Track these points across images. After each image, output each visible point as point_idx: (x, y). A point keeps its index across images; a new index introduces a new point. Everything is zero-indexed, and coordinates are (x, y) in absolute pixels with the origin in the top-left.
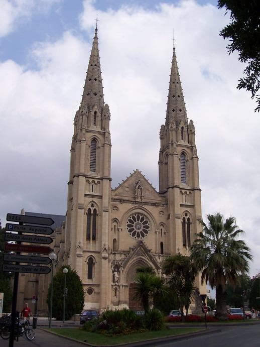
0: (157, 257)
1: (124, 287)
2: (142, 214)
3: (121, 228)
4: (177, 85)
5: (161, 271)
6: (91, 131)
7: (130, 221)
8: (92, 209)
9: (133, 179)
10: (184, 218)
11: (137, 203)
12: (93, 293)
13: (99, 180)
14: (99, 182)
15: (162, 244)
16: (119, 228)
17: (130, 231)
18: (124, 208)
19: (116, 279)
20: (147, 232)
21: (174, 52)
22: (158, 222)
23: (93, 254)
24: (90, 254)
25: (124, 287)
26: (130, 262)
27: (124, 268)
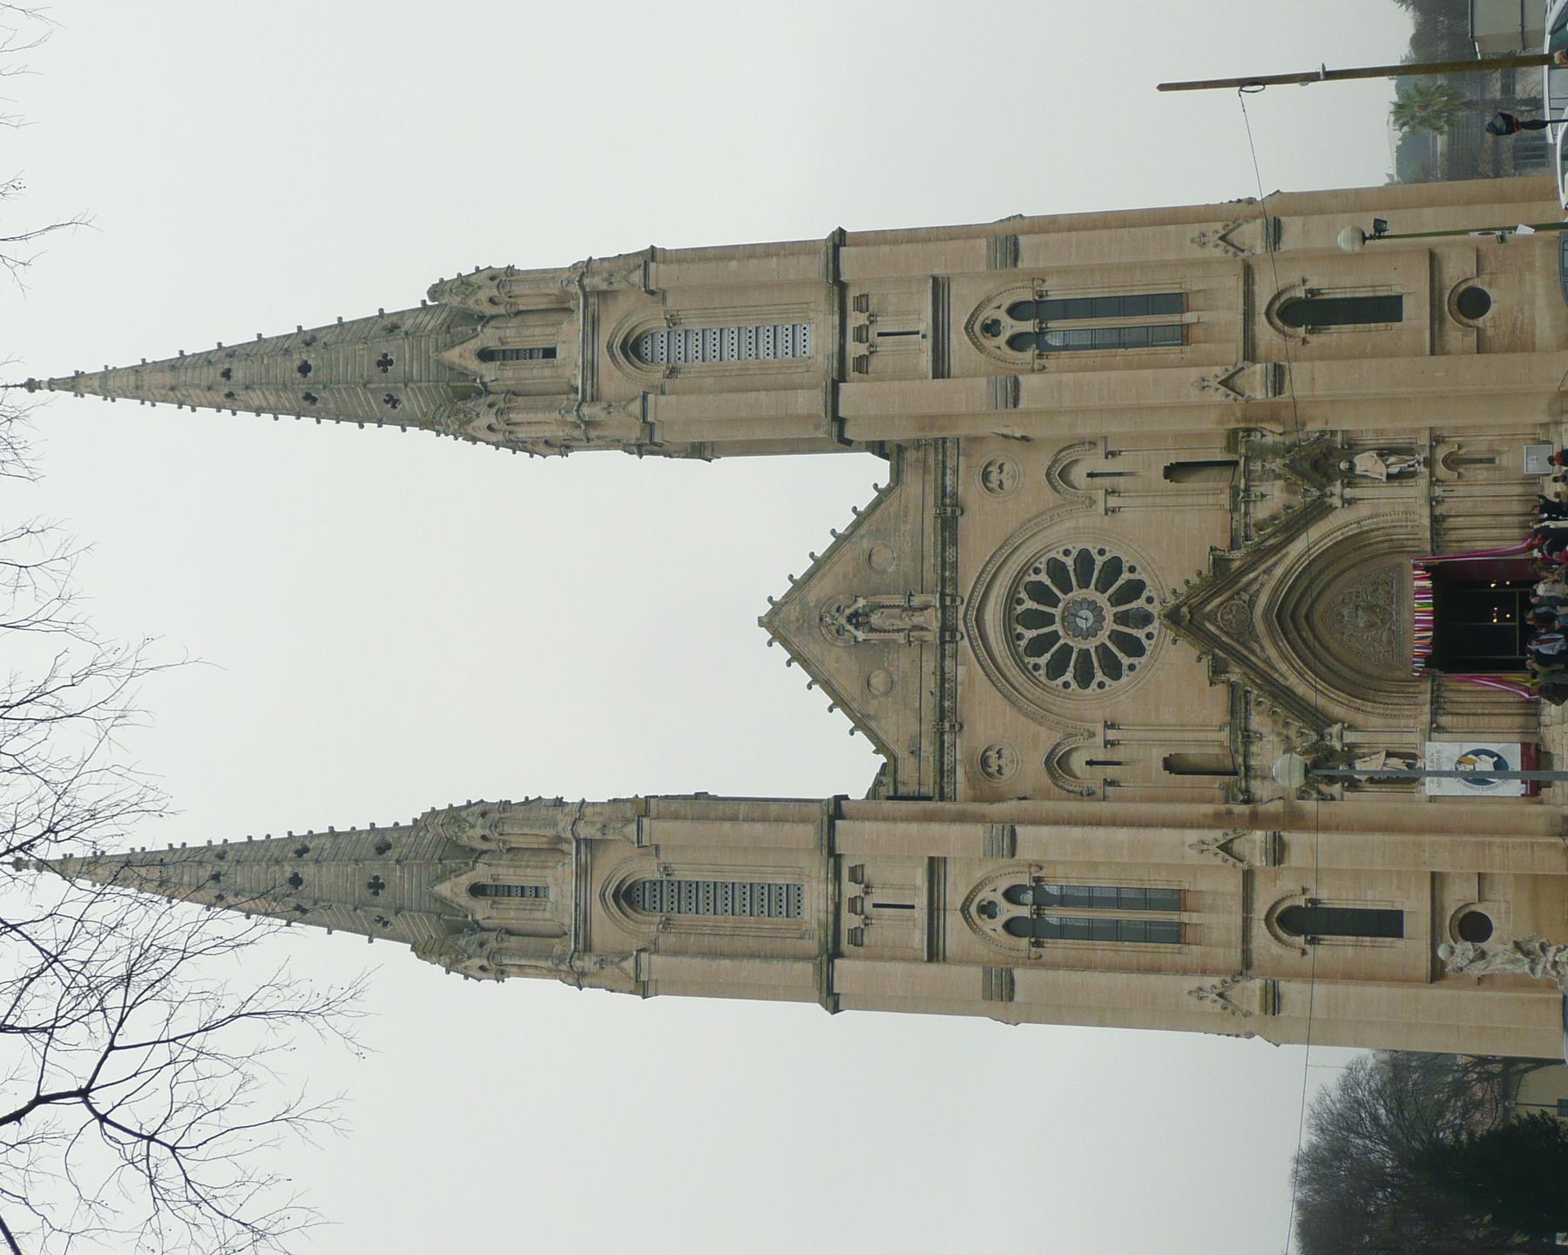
0: (1261, 512)
1: (1444, 720)
2: (1012, 599)
4: (238, 374)
5: (1337, 488)
6: (583, 919)
7: (1056, 669)
9: (813, 650)
10: (1016, 342)
11: (948, 631)
12: (1479, 908)
13: (845, 874)
14: (853, 870)
15: (1174, 472)
16: (1099, 740)
17: (1114, 670)
18: (989, 718)
21: (53, 384)
22: (1050, 498)
23: (1261, 909)
24: (1260, 930)
25: (1444, 720)
26: (1293, 681)
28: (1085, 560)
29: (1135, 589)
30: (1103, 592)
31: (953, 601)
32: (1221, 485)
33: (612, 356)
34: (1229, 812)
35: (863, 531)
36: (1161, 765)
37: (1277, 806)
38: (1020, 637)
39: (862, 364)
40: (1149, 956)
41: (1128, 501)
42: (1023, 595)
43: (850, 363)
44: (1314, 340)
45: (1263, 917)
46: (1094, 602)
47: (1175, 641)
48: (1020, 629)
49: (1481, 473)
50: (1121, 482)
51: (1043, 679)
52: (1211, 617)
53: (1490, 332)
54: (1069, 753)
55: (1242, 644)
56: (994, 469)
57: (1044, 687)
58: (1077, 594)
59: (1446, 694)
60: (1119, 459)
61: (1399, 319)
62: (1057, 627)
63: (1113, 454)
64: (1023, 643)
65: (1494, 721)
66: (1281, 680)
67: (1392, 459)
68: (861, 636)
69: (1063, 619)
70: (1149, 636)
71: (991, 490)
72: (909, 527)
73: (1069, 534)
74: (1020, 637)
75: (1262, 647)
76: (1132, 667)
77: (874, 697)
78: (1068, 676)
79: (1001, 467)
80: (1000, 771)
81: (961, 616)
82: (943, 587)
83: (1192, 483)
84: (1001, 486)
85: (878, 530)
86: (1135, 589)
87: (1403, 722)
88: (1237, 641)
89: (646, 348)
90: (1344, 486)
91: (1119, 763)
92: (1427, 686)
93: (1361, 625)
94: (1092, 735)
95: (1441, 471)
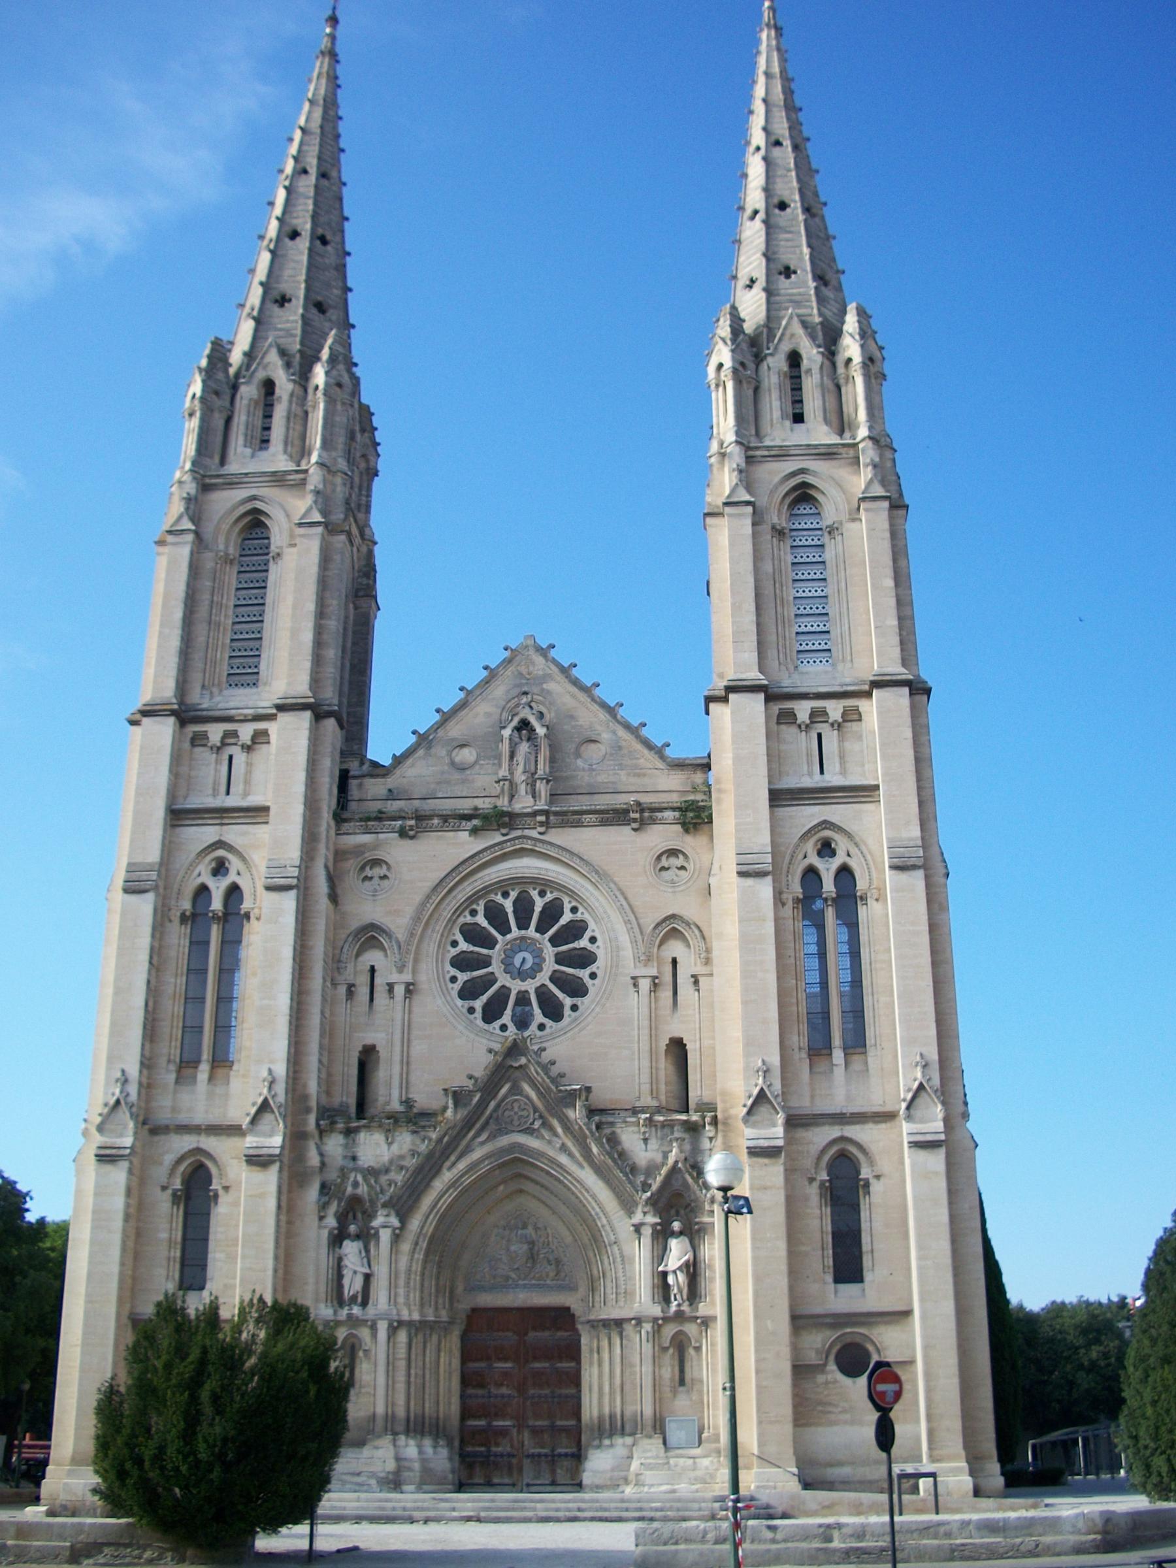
0: (630, 1138)
2: (544, 885)
3: (407, 977)
5: (652, 1219)
7: (473, 934)
8: (218, 888)
9: (500, 690)
15: (678, 1048)
16: (394, 977)
17: (468, 992)
19: (352, 1285)
20: (577, 990)
25: (402, 1336)
26: (447, 1176)
27: (403, 1218)
28: (585, 959)
29: (553, 1011)
30: (551, 979)
31: (542, 824)
32: (663, 1098)
33: (793, 474)
34: (308, 1110)
35: (622, 732)
36: (369, 1042)
37: (314, 1160)
38: (506, 895)
39: (787, 717)
40: (167, 1030)
41: (646, 1000)
42: (549, 897)
43: (788, 705)
44: (813, 1191)
45: (203, 1146)
46: (541, 970)
47: (490, 1051)
48: (513, 894)
49: (668, 1371)
50: (666, 994)
51: (462, 920)
52: (516, 1090)
53: (821, 1378)
54: (383, 949)
55: (487, 1123)
56: (680, 861)
57: (452, 921)
58: (549, 952)
59: (435, 1338)
60: (691, 988)
61: (837, 1280)
62: (515, 932)
63: (696, 982)
64: (499, 898)
65: (401, 1387)
66: (448, 1164)
67: (681, 1277)
68: (506, 733)
69: (523, 939)
70: (504, 1028)
71: (659, 858)
72: (624, 778)
73: (612, 937)
74: (506, 895)
75: (483, 1143)
76: (471, 1010)
77: (450, 753)
78: (463, 946)
79: (683, 868)
80: (366, 878)
81: (527, 832)
82: (556, 814)
83: (665, 1067)
84: (663, 869)
85: (620, 748)
86: (553, 1011)
87: (401, 1291)
88: (490, 1117)
89: (805, 509)
90: (654, 1226)
91: (372, 999)
92: (444, 1316)
93: (513, 1248)
94: (401, 970)
95: (670, 1330)
